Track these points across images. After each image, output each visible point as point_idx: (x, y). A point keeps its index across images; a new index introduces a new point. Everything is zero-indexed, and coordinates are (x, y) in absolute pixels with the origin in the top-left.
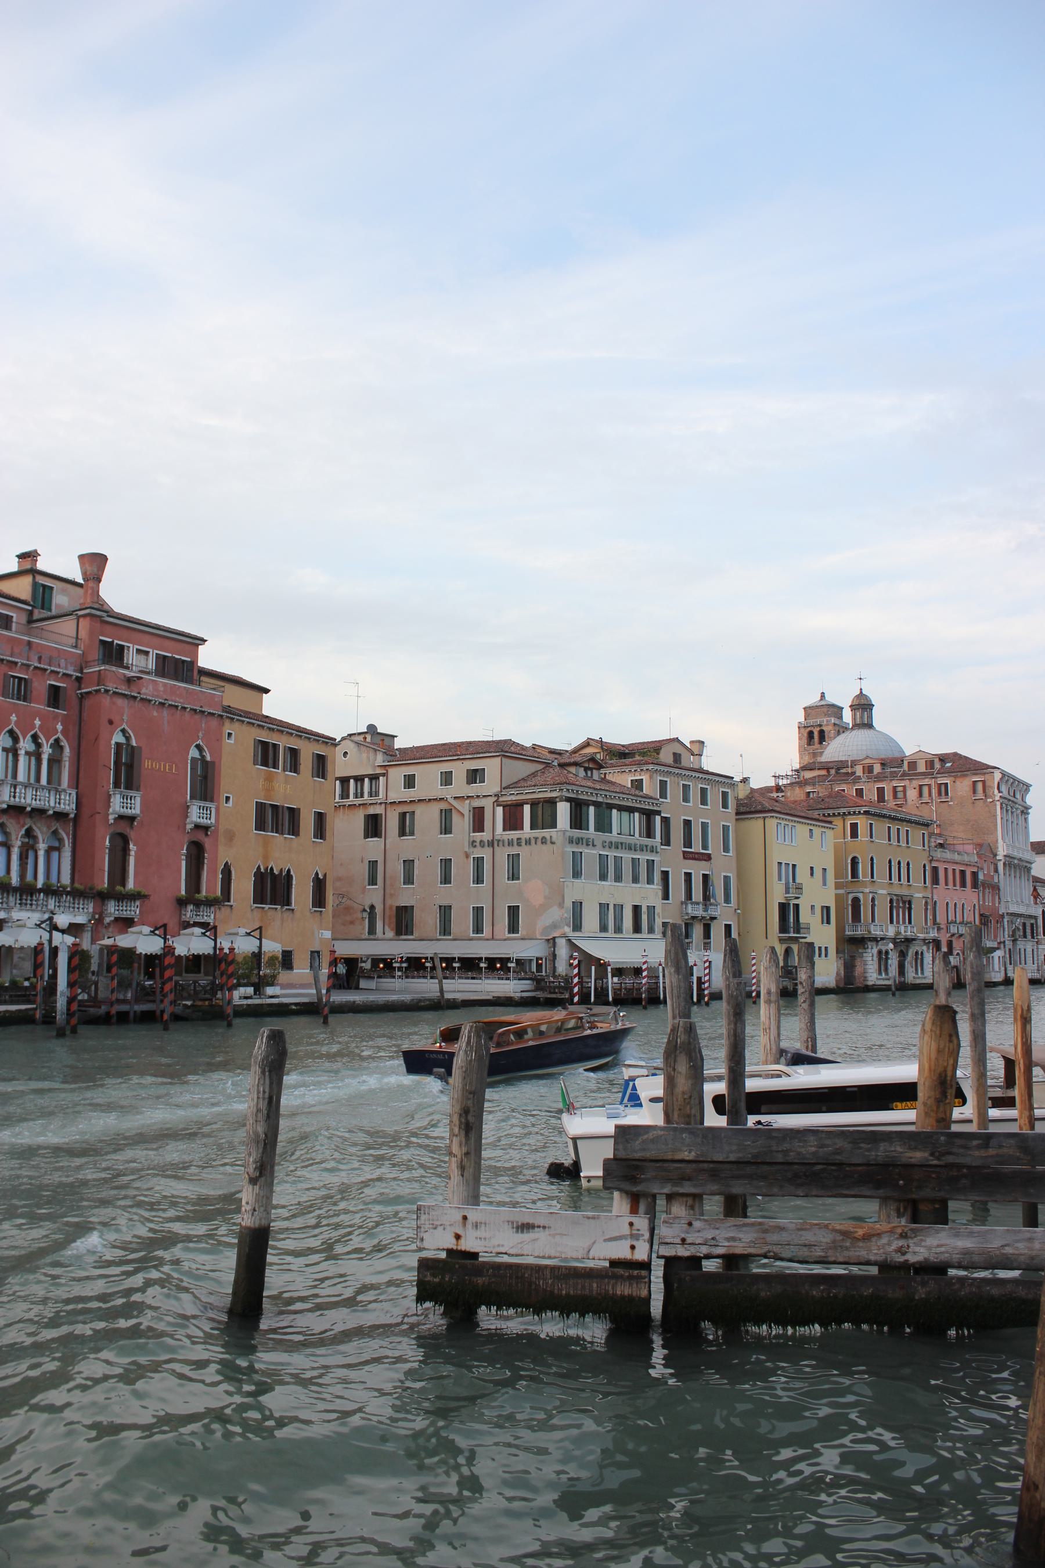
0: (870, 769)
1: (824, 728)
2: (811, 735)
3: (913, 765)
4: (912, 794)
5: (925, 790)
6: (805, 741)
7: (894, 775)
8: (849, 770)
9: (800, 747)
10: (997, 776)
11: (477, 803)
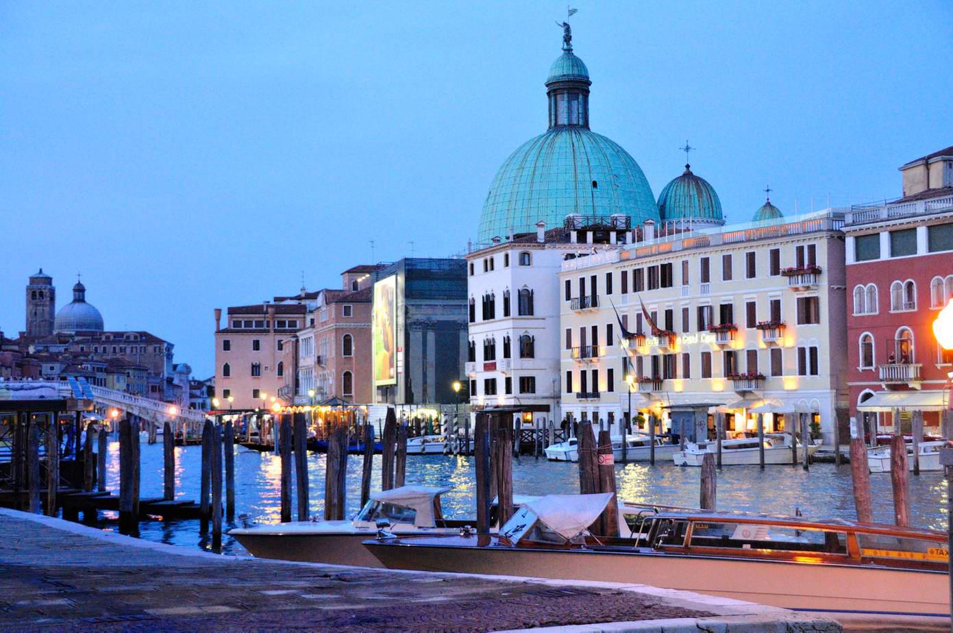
0: (108, 338)
3: (128, 337)
4: (128, 351)
5: (134, 350)
7: (120, 342)
8: (99, 337)
9: (27, 300)
10: (166, 345)
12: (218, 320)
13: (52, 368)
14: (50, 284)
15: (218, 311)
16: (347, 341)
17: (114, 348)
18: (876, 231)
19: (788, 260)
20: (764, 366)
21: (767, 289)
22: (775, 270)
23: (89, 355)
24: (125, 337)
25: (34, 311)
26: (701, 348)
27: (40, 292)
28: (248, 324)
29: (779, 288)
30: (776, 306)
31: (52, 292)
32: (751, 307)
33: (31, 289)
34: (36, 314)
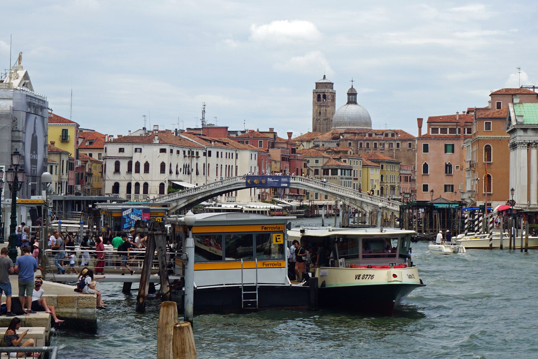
0: (370, 135)
1: (326, 94)
2: (319, 96)
3: (387, 135)
4: (387, 146)
6: (316, 99)
11: (316, 168)
12: (420, 127)
13: (317, 162)
14: (332, 88)
15: (420, 121)
16: (488, 149)
17: (375, 144)
23: (347, 151)
24: (384, 134)
25: (318, 112)
27: (323, 95)
28: (444, 131)
31: (333, 94)
33: (317, 93)
34: (320, 113)
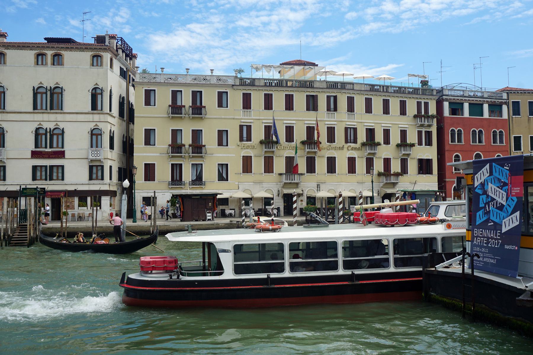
18: (462, 102)
19: (412, 108)
20: (396, 167)
21: (396, 122)
22: (403, 112)
26: (384, 154)
29: (406, 123)
30: (403, 133)
32: (387, 133)
